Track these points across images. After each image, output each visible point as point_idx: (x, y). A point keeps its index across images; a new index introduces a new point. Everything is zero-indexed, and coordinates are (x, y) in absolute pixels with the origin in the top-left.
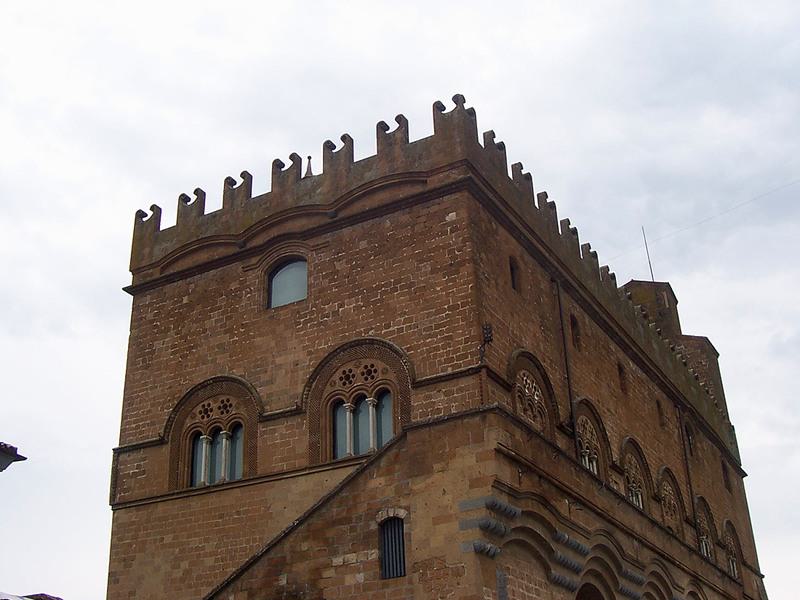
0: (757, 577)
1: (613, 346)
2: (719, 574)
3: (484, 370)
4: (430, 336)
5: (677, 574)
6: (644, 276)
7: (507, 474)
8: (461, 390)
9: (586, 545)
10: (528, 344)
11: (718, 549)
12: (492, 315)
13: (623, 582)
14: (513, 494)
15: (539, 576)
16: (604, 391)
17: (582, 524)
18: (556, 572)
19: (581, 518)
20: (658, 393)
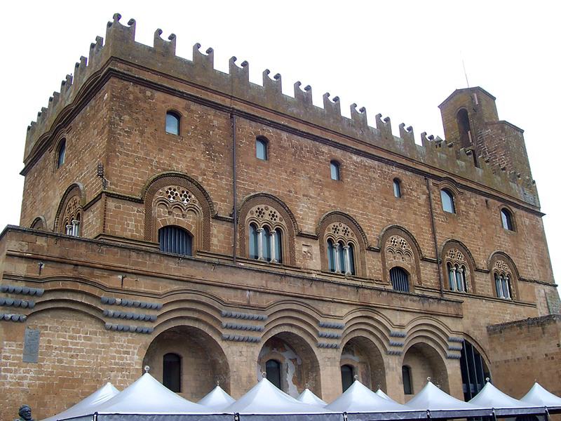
0: (548, 288)
1: (325, 149)
2: (418, 299)
3: (104, 194)
4: (93, 176)
5: (324, 308)
6: (464, 86)
7: (21, 268)
8: (97, 209)
9: (156, 303)
10: (181, 167)
11: (476, 273)
12: (127, 155)
13: (225, 322)
14: (27, 279)
15: (90, 326)
16: (302, 182)
17: (143, 289)
18: (109, 323)
19: (144, 285)
20: (397, 172)
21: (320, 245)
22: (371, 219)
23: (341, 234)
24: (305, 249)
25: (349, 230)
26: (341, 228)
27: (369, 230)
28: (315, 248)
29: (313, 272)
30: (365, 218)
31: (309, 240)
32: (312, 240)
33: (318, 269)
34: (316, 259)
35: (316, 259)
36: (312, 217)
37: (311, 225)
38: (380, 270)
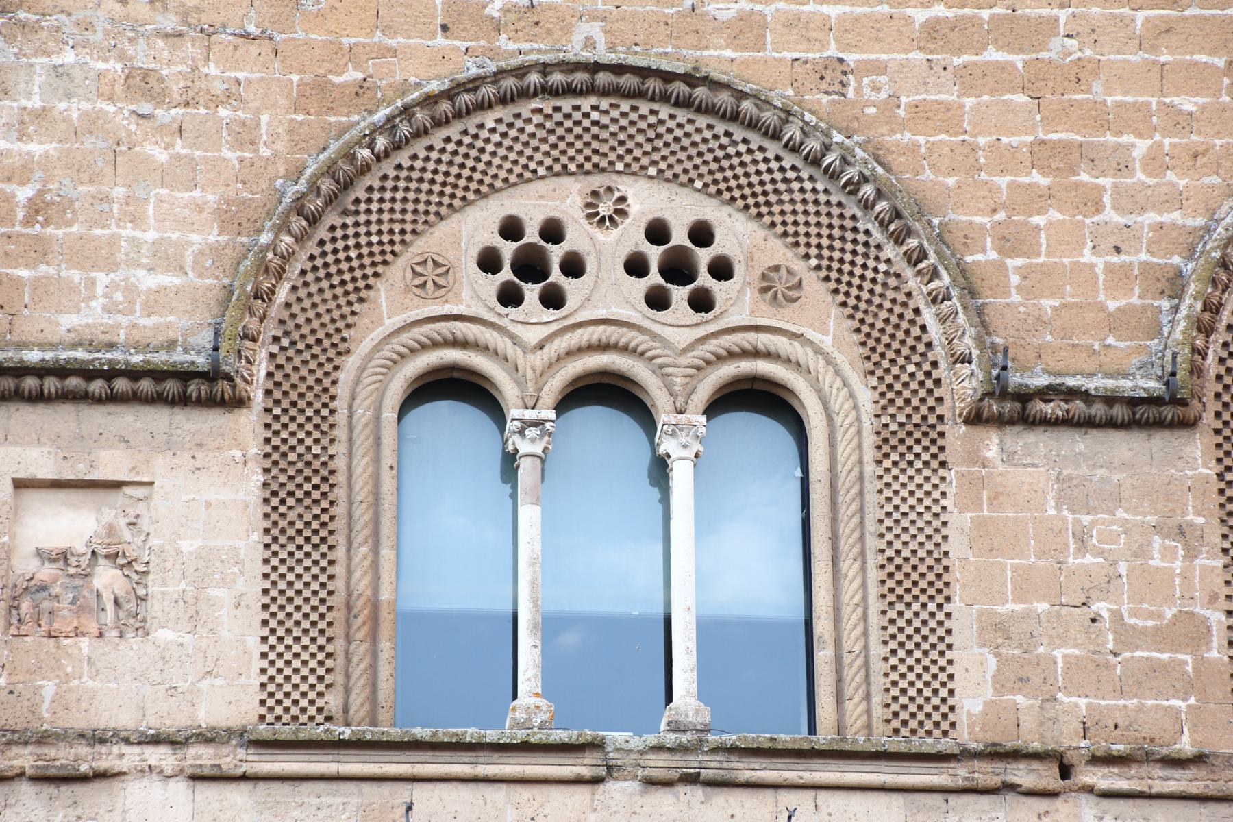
21: (275, 456)
22: (1078, 76)
23: (607, 294)
24: (67, 524)
25: (736, 234)
26: (604, 249)
27: (1045, 198)
28: (200, 493)
29: (131, 757)
30: (968, 78)
31: (128, 419)
32: (158, 419)
33: (208, 715)
34: (194, 613)
35: (194, 613)
36: (182, 174)
37: (164, 257)
38: (1189, 632)
